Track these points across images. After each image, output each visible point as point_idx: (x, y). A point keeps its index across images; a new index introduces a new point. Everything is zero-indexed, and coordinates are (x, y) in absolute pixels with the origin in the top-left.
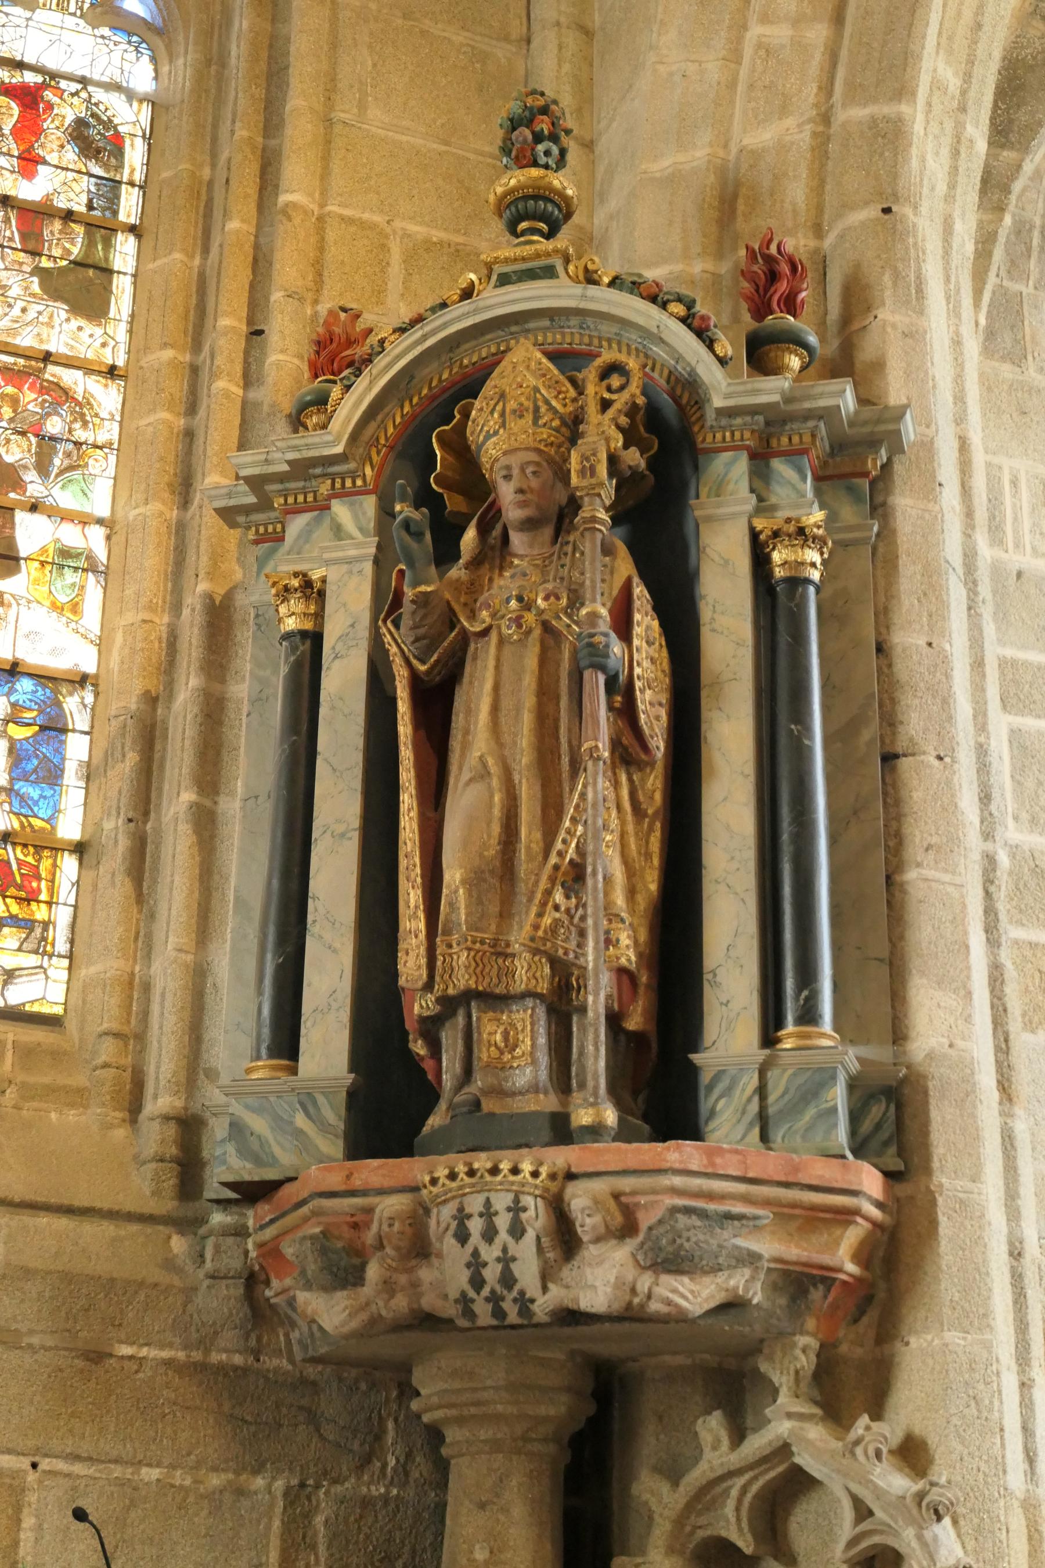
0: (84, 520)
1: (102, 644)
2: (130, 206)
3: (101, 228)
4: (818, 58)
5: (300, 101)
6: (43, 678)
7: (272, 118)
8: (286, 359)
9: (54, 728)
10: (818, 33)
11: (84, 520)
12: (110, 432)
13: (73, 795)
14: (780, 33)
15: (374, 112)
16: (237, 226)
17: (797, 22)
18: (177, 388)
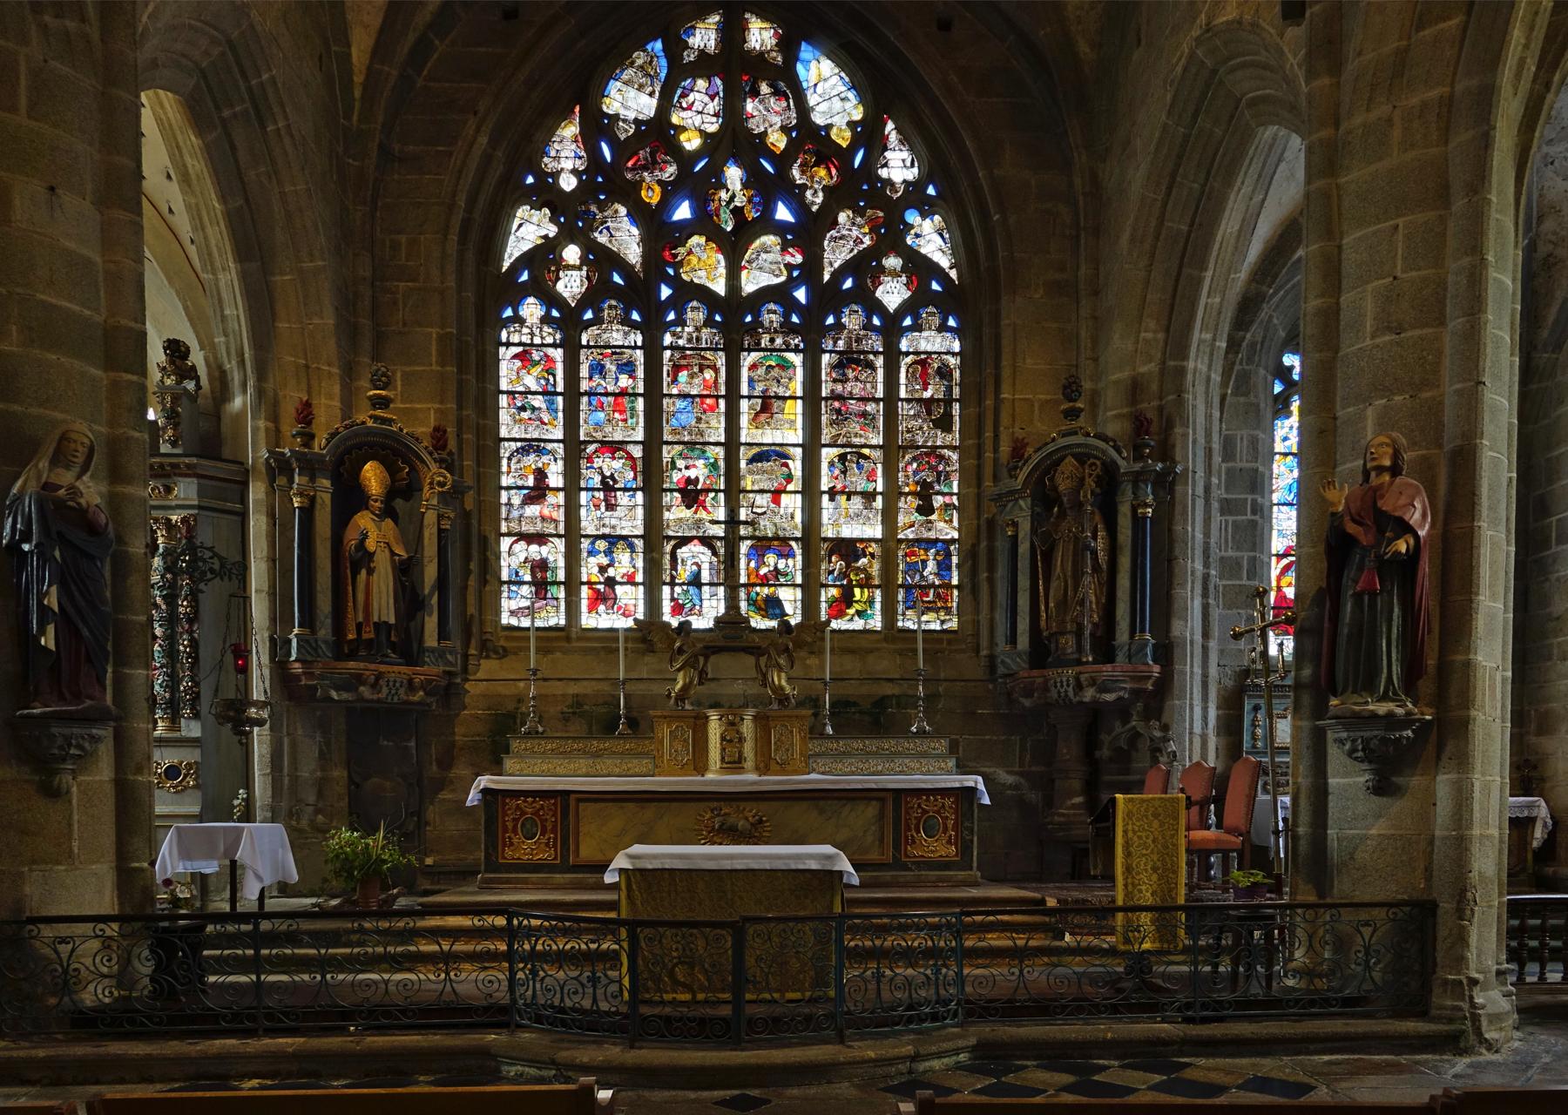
0: (952, 494)
1: (959, 530)
2: (956, 392)
3: (948, 401)
4: (1161, 344)
5: (1005, 362)
6: (944, 541)
7: (997, 366)
8: (1005, 449)
9: (949, 555)
10: (1161, 336)
11: (952, 494)
12: (957, 466)
13: (955, 574)
14: (1149, 335)
15: (1028, 361)
16: (989, 402)
17: (1155, 332)
18: (974, 452)
